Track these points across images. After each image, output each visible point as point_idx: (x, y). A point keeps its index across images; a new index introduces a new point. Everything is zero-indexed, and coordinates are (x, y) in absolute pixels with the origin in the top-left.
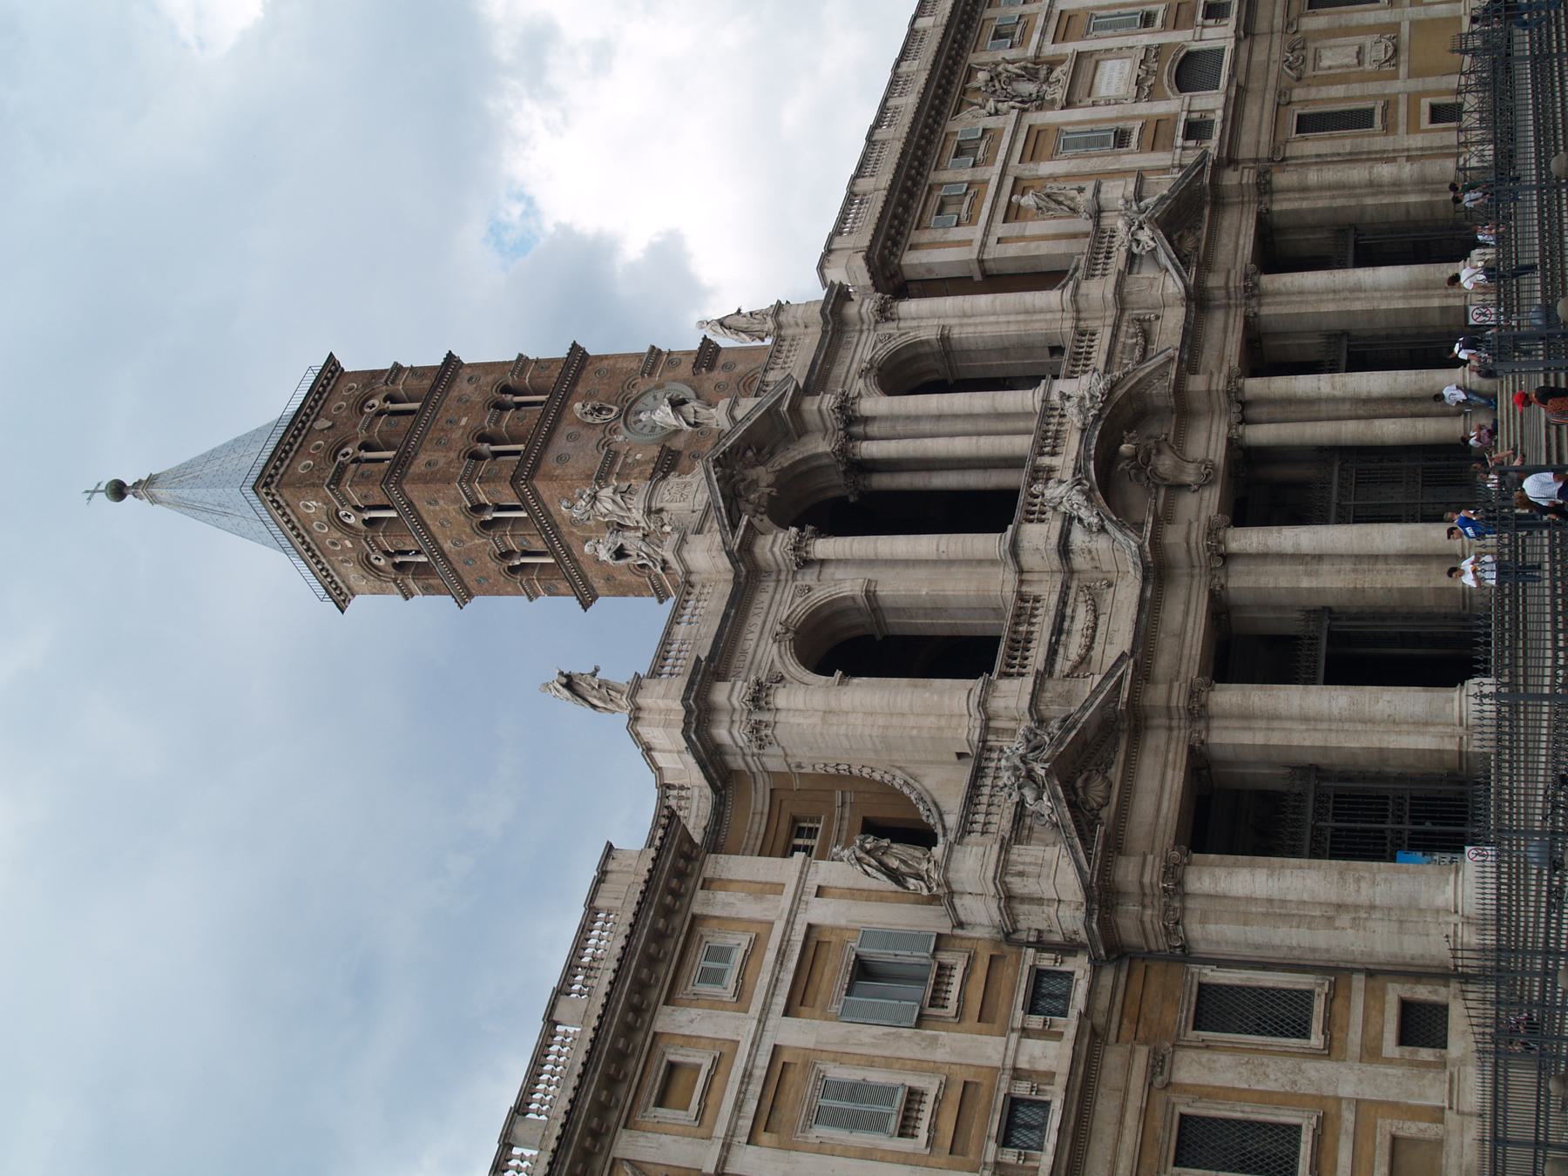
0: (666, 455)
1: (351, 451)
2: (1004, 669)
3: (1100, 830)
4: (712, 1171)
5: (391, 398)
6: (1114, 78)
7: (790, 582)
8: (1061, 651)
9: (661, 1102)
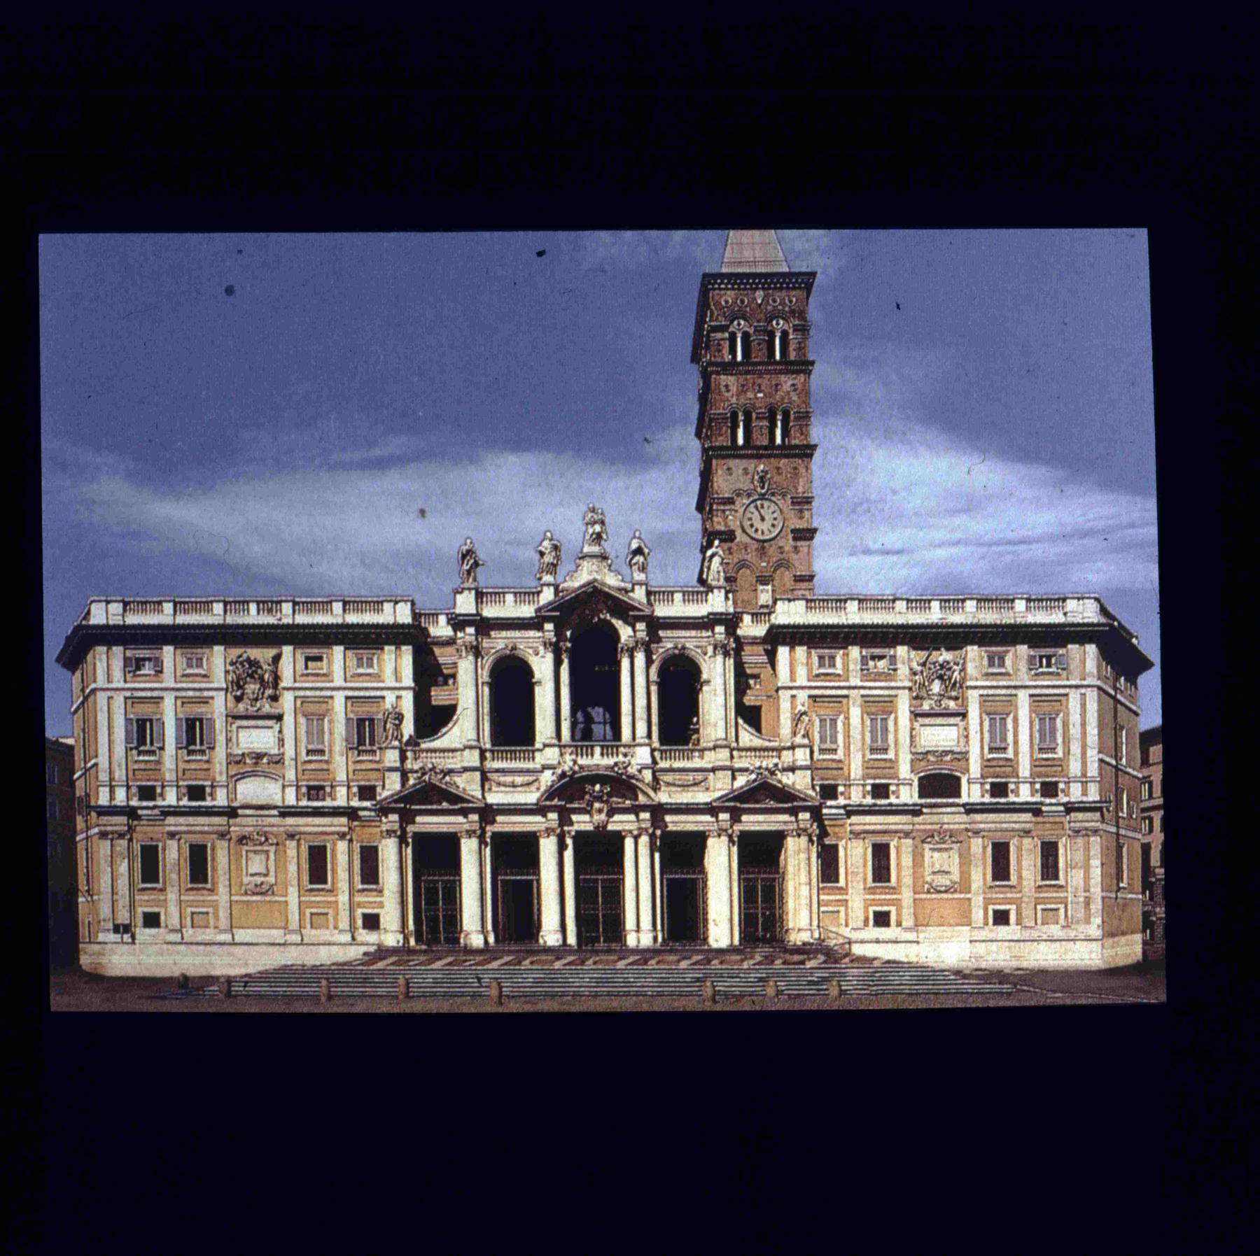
6: (940, 736)
9: (308, 659)
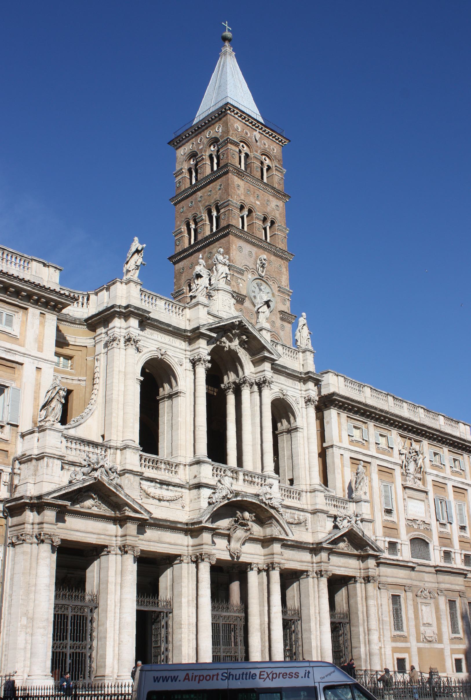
0: (241, 298)
1: (244, 149)
2: (144, 457)
3: (68, 503)
5: (269, 168)
7: (185, 356)
8: (153, 484)
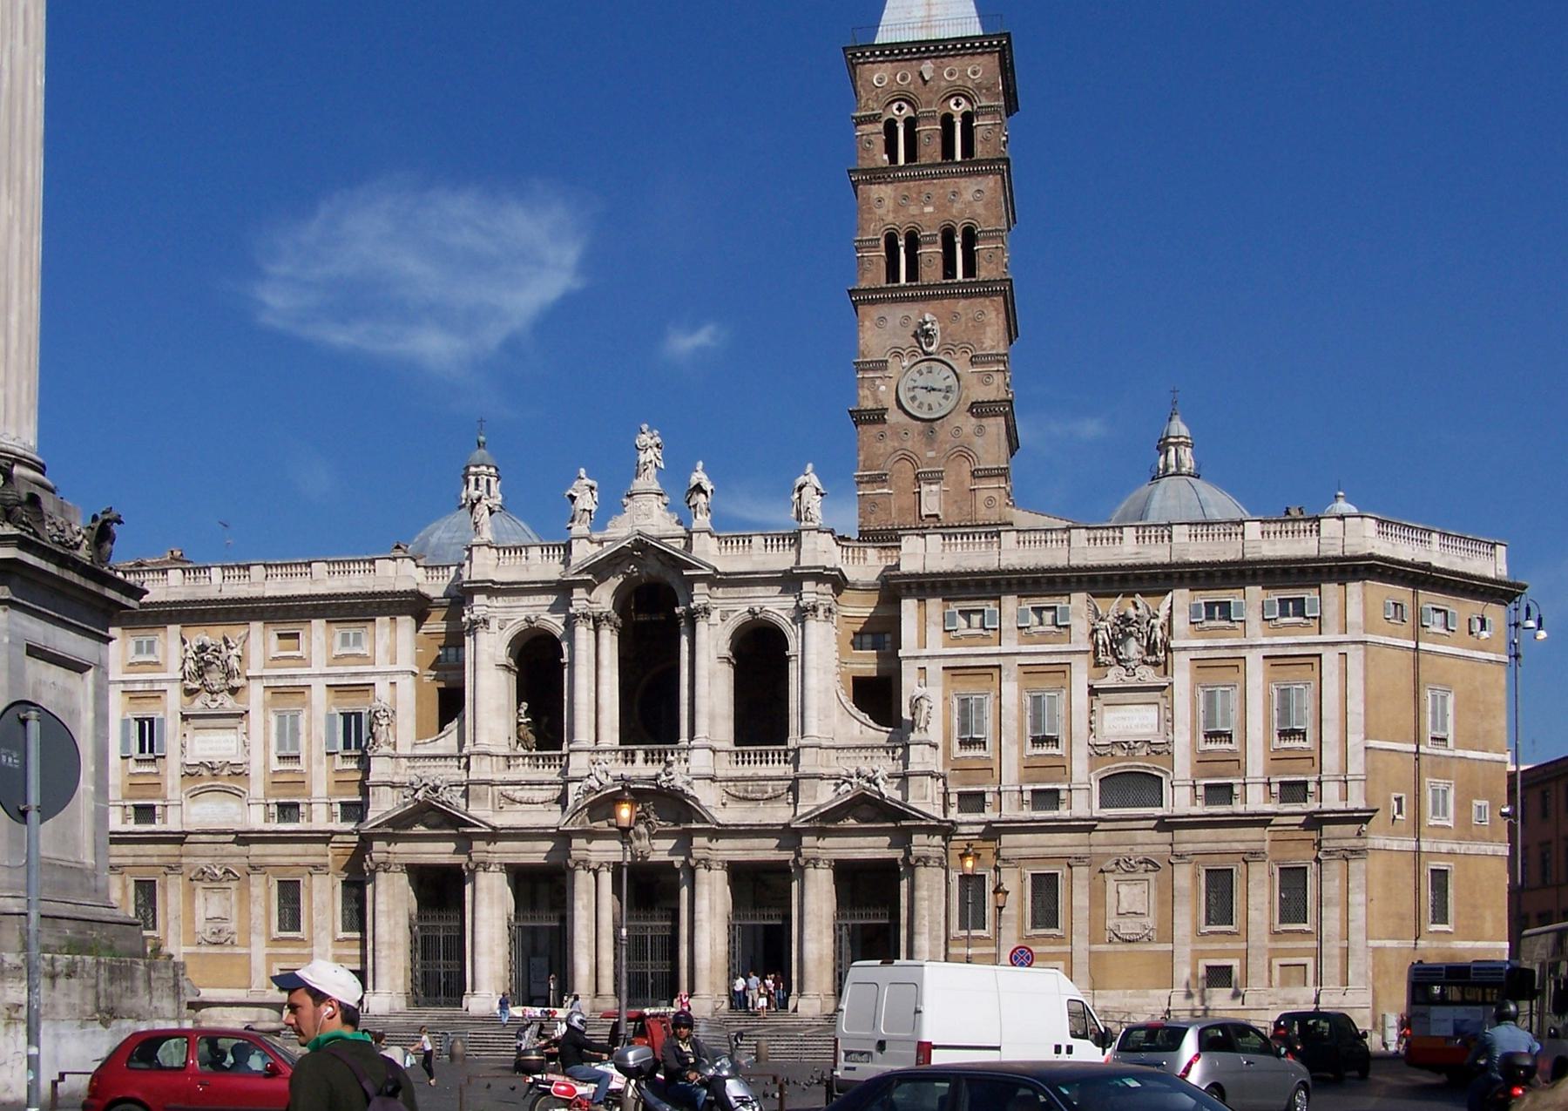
1: (903, 112)
3: (390, 830)
4: (248, 674)
5: (968, 118)
8: (519, 787)
9: (280, 636)
